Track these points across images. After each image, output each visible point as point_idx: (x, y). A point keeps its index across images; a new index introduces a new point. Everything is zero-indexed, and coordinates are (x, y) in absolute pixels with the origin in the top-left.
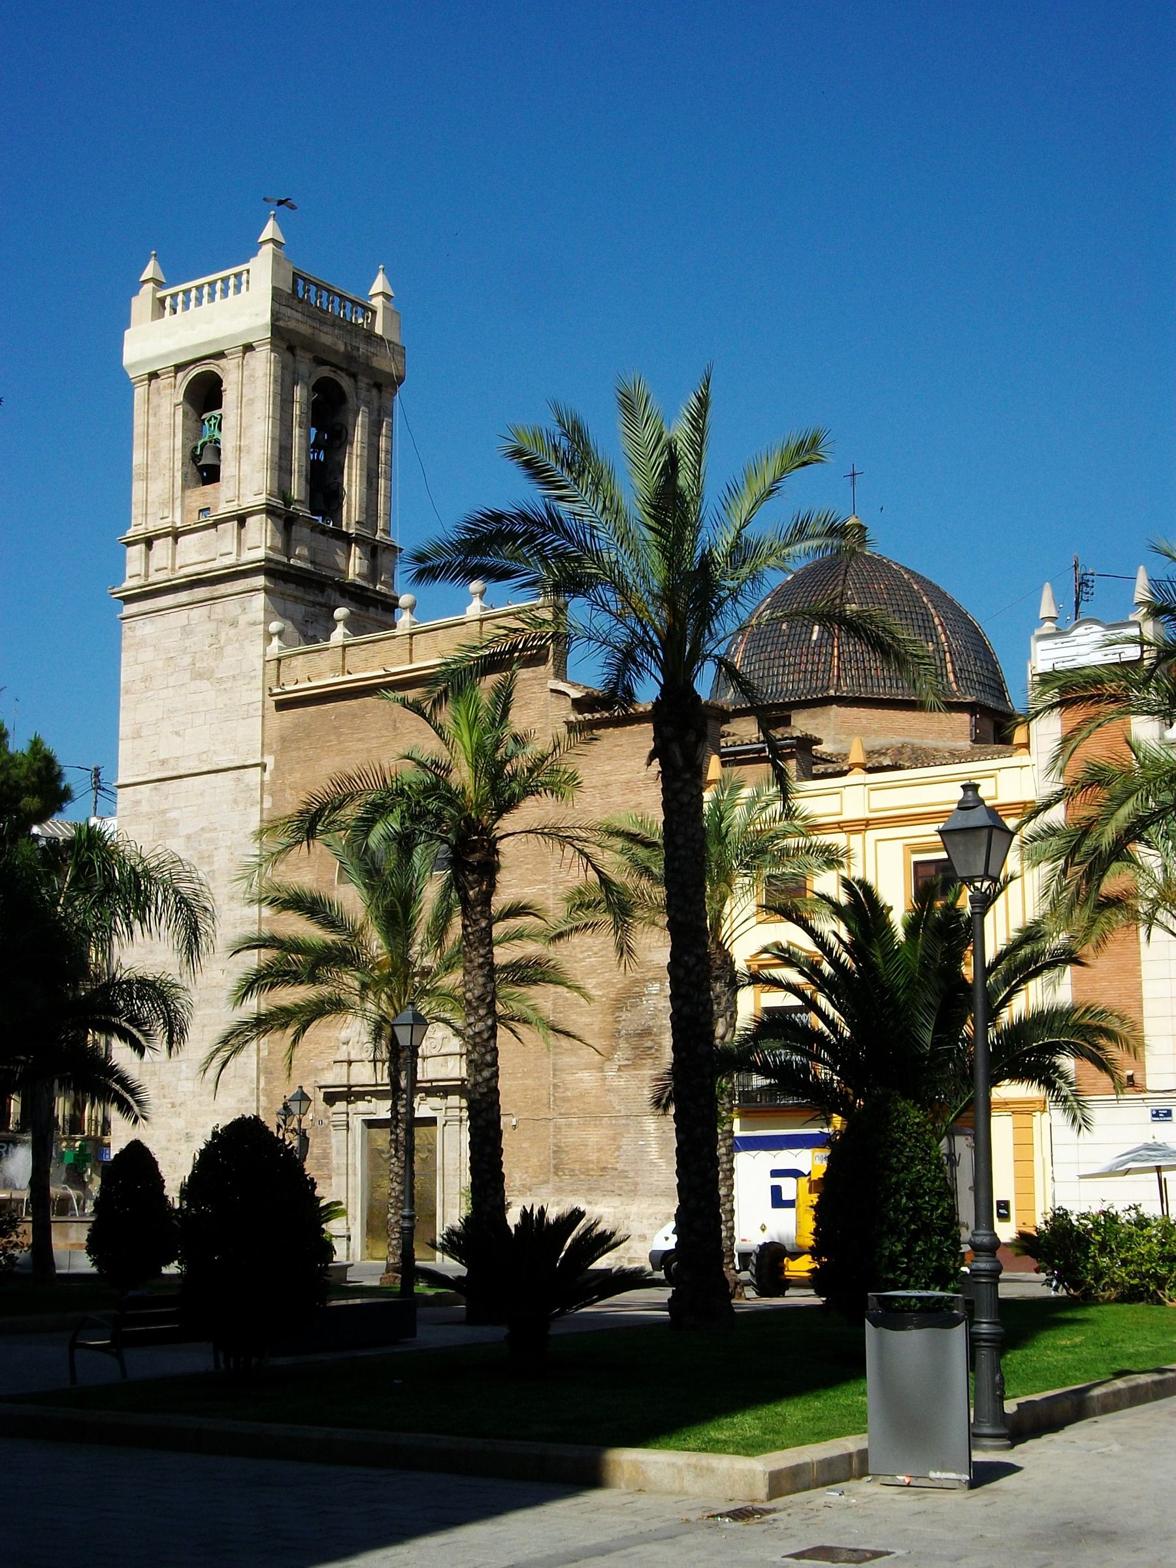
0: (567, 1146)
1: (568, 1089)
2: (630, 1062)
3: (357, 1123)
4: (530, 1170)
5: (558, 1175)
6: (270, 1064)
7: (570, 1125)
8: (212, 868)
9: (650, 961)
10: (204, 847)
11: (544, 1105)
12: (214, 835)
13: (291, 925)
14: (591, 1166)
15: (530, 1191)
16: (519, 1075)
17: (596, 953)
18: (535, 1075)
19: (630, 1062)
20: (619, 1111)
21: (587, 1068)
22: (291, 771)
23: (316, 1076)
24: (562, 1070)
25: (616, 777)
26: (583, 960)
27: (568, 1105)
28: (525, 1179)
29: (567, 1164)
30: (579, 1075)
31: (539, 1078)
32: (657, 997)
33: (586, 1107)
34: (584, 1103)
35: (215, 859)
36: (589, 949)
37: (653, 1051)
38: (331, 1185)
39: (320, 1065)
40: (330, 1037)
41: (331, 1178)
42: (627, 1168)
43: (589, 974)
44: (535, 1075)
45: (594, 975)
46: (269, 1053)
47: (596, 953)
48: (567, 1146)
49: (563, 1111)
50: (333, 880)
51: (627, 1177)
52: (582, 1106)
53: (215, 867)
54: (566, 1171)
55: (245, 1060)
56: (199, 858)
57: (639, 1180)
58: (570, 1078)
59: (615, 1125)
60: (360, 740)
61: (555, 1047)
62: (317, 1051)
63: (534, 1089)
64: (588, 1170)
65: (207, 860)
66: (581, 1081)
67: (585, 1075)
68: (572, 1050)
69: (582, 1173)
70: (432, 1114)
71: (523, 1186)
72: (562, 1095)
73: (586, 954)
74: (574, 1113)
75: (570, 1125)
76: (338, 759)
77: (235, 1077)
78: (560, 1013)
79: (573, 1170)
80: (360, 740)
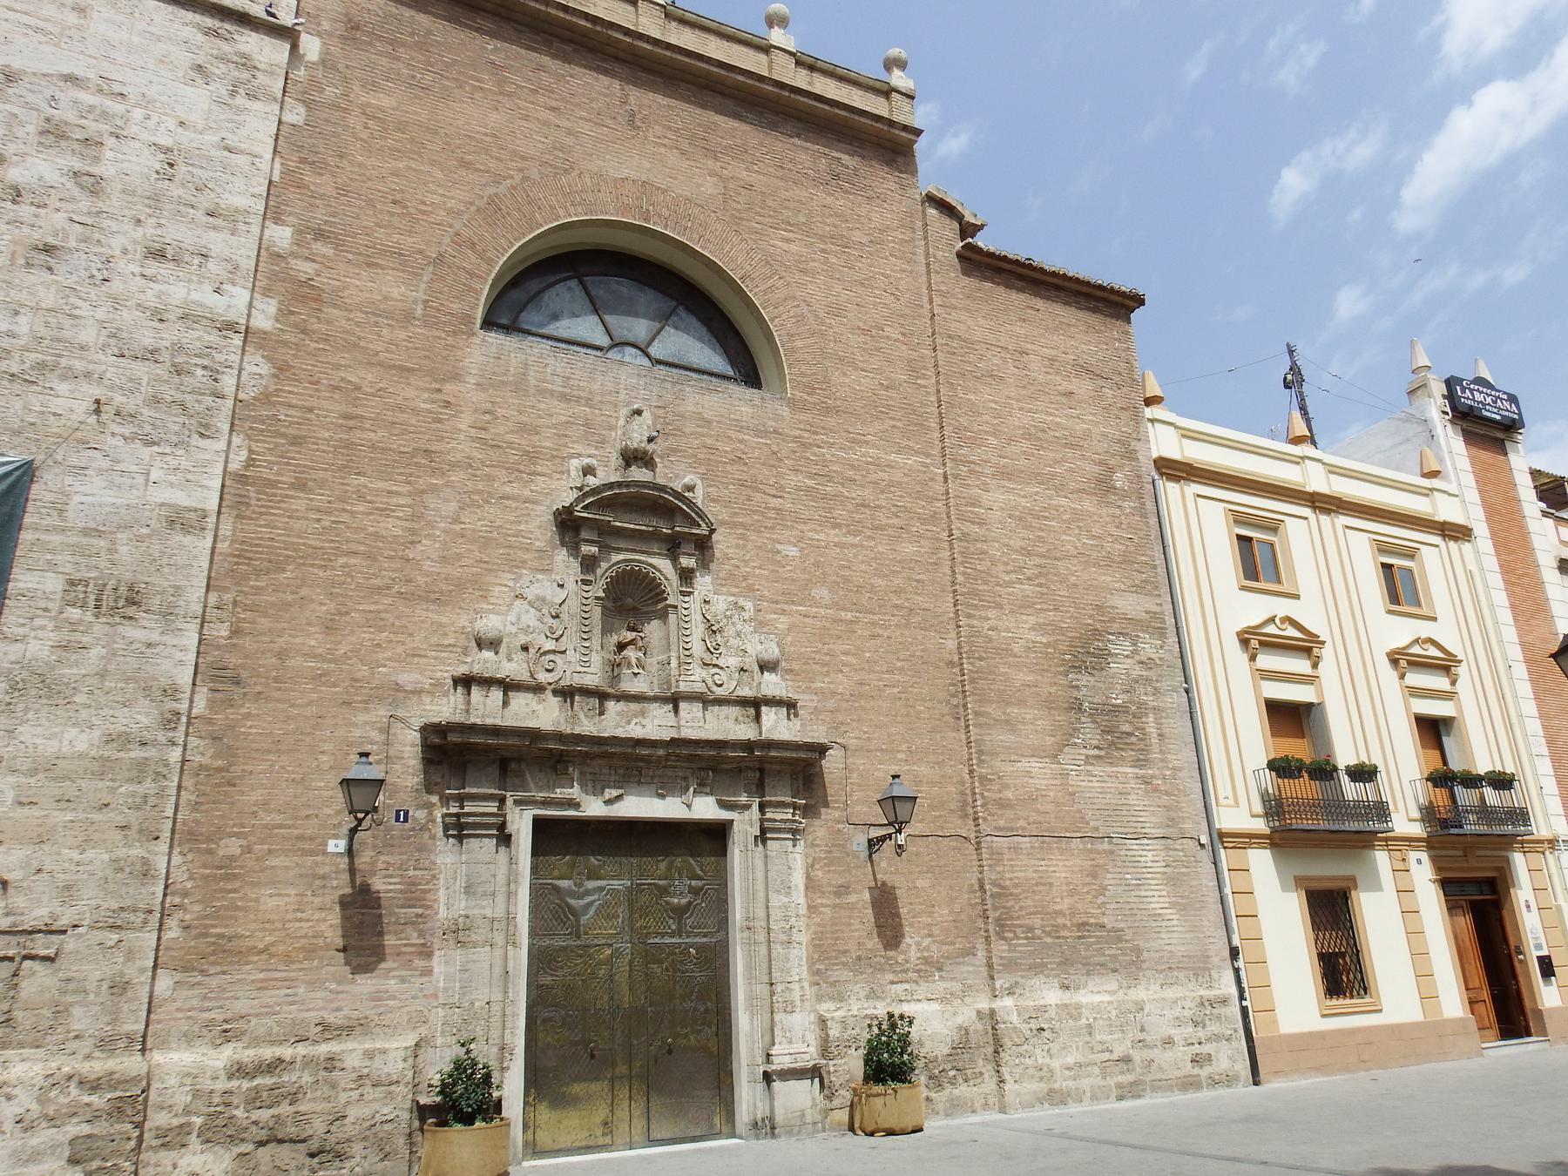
0: (1016, 886)
1: (1007, 787)
2: (1102, 753)
3: (521, 824)
4: (936, 930)
5: (1005, 939)
6: (233, 660)
7: (1016, 849)
8: (95, 170)
9: (1113, 607)
10: (71, 116)
11: (952, 811)
12: (117, 107)
13: (337, 367)
14: (1060, 921)
15: (940, 969)
16: (901, 756)
17: (1029, 579)
18: (932, 758)
19: (1102, 753)
20: (1097, 829)
21: (1036, 753)
22: (371, 86)
23: (394, 704)
24: (994, 754)
25: (1034, 347)
26: (1009, 584)
27: (1009, 814)
28: (927, 949)
29: (1018, 918)
30: (1025, 764)
31: (940, 764)
32: (1129, 661)
33: (1040, 818)
34: (1038, 812)
35: (109, 154)
36: (1019, 570)
37: (1133, 739)
38: (428, 972)
39: (407, 678)
40: (441, 625)
41: (429, 955)
42: (1123, 925)
43: (1021, 607)
44: (932, 758)
45: (1031, 611)
46: (235, 632)
47: (1029, 579)
48: (1016, 886)
49: (1002, 823)
50: (468, 320)
51: (1120, 939)
52: (1034, 817)
53: (106, 169)
54: (1018, 930)
55: (155, 637)
56: (42, 133)
57: (1142, 944)
58: (1008, 768)
59: (1091, 851)
60: (552, 109)
61: (976, 714)
62: (400, 649)
63: (933, 783)
64: (1057, 928)
65: (76, 146)
66: (1028, 774)
67: (1034, 765)
68: (1007, 722)
69: (1048, 934)
70: (724, 815)
71: (926, 961)
72: (996, 796)
73: (1014, 576)
74: (1023, 829)
75: (1016, 849)
76: (494, 116)
77: (103, 674)
78: (981, 659)
79: (1031, 929)
80: (552, 109)
